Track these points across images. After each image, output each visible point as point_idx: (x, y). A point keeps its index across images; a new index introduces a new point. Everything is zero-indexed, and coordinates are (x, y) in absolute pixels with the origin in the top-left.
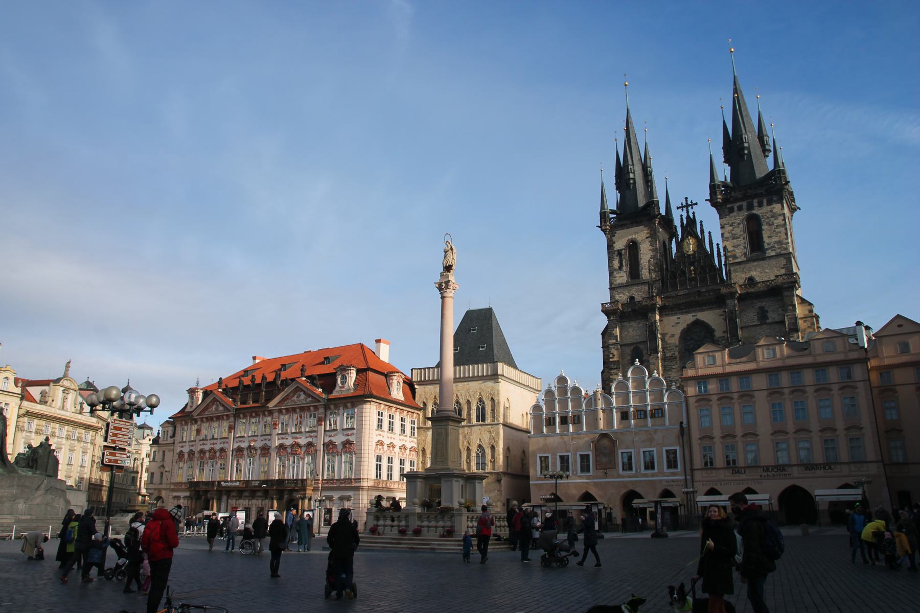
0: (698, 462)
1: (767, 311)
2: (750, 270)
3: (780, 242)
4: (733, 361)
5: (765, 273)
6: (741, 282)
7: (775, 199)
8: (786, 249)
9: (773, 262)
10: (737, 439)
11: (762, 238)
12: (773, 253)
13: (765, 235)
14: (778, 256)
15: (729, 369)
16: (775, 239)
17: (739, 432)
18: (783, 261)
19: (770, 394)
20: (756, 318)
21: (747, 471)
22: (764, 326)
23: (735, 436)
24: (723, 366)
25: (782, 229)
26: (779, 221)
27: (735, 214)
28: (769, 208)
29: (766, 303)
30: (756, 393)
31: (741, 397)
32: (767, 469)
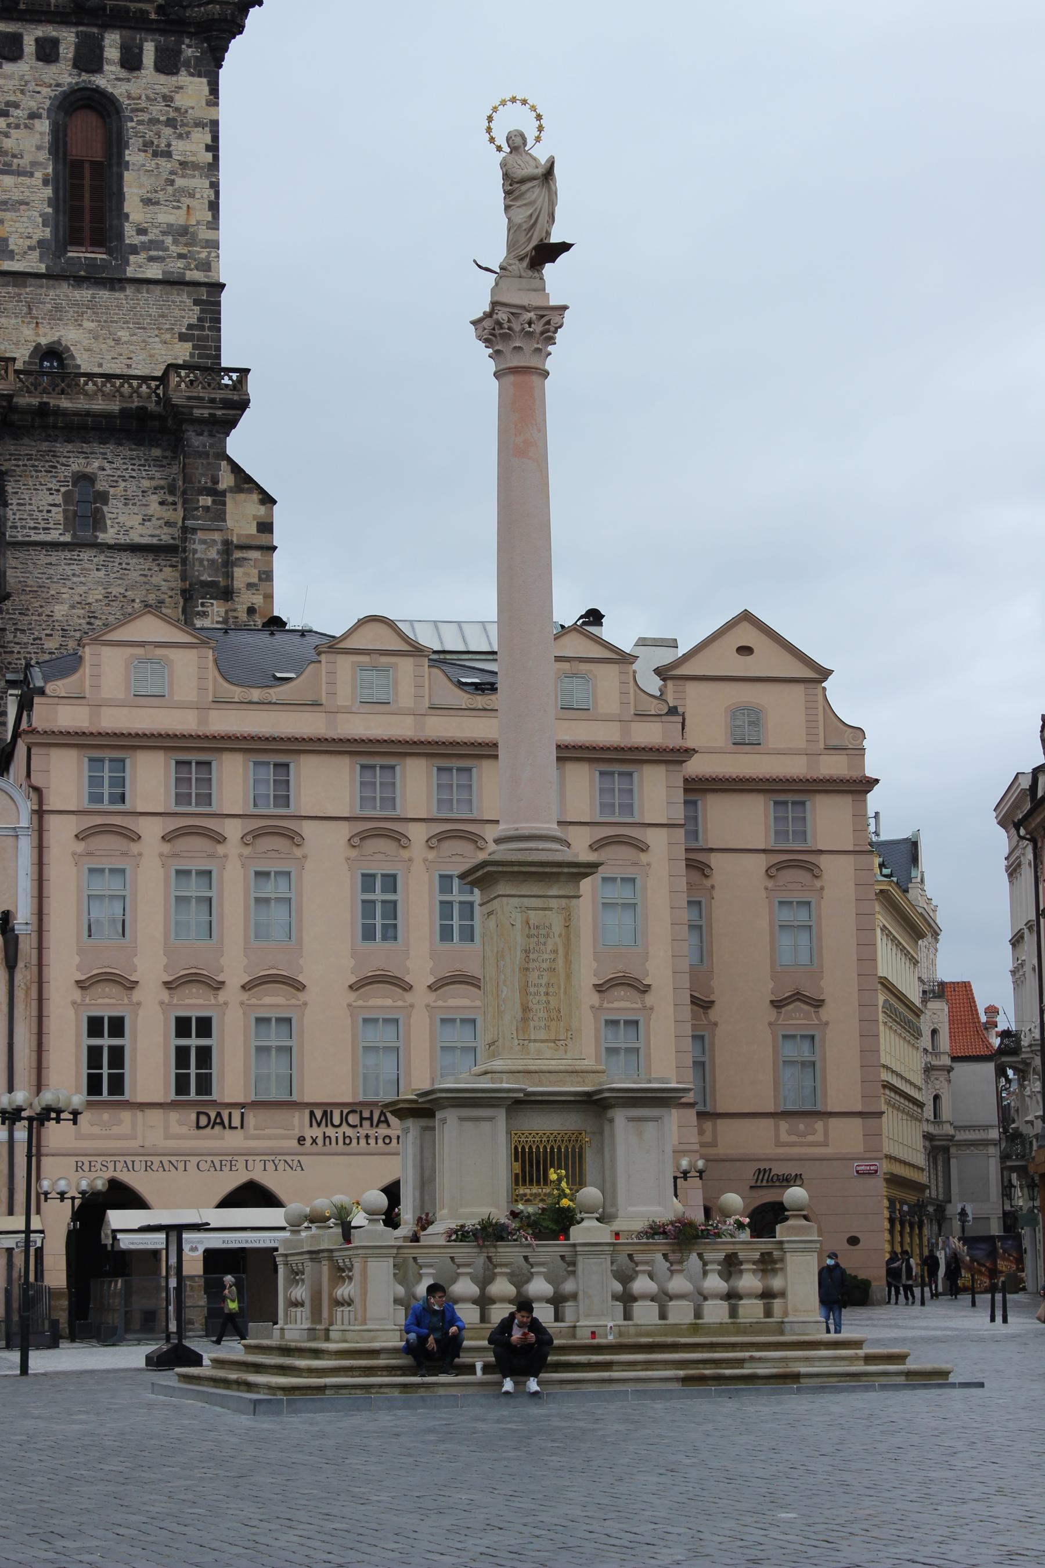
1: (103, 497)
2: (57, 313)
3: (182, 232)
4: (237, 693)
5: (117, 342)
6: (22, 355)
7: (189, 52)
8: (206, 266)
9: (149, 302)
10: (222, 996)
11: (120, 197)
12: (154, 272)
13: (134, 187)
14: (173, 282)
16: (167, 216)
17: (234, 971)
18: (185, 311)
20: (58, 514)
21: (251, 1118)
22: (86, 555)
23: (407, 988)
25: (200, 183)
26: (194, 146)
27: (25, 67)
28: (165, 82)
29: (110, 466)
30: (307, 828)
32: (322, 1114)
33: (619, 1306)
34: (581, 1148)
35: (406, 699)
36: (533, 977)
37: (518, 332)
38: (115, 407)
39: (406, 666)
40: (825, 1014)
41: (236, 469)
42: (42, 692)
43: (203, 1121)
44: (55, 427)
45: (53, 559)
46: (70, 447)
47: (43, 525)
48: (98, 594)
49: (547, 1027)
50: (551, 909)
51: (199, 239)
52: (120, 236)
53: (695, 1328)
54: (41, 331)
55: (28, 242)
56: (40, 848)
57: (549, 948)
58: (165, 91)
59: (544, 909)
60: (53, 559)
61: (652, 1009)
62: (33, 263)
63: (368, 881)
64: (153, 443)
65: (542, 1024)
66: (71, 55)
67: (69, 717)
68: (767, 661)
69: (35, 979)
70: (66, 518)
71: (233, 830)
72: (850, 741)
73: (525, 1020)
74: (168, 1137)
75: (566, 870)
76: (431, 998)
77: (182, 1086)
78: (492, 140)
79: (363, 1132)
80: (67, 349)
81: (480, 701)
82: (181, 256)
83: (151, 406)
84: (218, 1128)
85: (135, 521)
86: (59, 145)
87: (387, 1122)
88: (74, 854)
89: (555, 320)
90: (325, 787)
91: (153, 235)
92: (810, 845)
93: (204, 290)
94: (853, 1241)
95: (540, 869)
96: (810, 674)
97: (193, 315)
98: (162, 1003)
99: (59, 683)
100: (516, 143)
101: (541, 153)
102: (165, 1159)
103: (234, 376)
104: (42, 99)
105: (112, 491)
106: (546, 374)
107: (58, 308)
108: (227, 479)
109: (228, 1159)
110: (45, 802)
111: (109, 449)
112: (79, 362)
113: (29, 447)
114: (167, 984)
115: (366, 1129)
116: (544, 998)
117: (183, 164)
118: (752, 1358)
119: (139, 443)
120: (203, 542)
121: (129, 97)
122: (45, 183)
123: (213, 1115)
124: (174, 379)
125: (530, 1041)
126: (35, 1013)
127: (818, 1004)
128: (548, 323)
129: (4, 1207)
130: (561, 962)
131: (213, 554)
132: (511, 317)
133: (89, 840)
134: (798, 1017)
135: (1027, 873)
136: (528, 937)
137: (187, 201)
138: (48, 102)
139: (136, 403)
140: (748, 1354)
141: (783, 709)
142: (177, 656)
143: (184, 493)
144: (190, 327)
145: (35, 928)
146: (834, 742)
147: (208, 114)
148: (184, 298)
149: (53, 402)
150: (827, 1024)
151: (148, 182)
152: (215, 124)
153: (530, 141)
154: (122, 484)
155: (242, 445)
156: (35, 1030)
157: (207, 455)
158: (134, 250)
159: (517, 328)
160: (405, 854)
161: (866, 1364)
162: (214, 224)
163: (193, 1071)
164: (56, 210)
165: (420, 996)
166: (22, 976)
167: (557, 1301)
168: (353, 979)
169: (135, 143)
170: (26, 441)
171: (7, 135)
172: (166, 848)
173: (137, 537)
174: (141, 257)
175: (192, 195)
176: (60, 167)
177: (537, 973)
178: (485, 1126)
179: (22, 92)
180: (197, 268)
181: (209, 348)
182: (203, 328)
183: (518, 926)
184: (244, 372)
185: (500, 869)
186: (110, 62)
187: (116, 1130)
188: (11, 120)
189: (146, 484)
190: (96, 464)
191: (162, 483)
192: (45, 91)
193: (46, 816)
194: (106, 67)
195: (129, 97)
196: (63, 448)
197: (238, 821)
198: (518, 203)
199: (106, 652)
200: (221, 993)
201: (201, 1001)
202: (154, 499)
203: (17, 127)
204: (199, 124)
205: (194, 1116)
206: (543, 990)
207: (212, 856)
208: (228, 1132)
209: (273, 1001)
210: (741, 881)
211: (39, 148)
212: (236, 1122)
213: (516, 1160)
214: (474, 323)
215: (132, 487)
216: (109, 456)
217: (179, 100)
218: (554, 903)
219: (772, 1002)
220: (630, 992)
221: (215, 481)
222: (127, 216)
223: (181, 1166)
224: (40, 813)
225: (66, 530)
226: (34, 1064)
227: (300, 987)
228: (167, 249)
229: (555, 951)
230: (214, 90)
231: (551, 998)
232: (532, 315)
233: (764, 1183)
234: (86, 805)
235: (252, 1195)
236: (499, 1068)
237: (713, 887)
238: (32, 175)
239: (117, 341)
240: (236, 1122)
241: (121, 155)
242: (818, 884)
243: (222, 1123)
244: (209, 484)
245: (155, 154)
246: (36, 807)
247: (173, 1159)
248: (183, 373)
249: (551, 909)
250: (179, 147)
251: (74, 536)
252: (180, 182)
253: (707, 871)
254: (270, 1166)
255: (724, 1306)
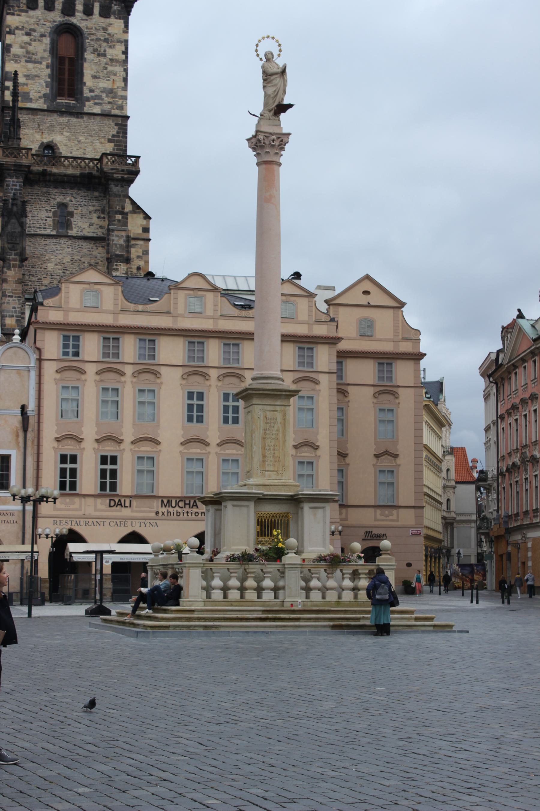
0: (50, 483)
1: (71, 214)
3: (111, 92)
4: (132, 307)
5: (78, 142)
6: (35, 147)
7: (115, 8)
8: (121, 108)
9: (94, 124)
10: (122, 446)
11: (82, 74)
12: (97, 110)
13: (88, 70)
15: (126, 320)
16: (103, 84)
17: (128, 434)
19: (186, 376)
20: (50, 221)
21: (134, 503)
22: (63, 241)
23: (207, 444)
24: (113, 313)
25: (119, 69)
26: (116, 52)
28: (103, 22)
29: (74, 200)
31: (137, 374)
32: (167, 501)
33: (304, 593)
34: (288, 520)
35: (209, 312)
36: (268, 442)
37: (267, 145)
38: (77, 172)
39: (210, 296)
40: (398, 461)
41: (133, 203)
42: (42, 304)
43: (112, 503)
44: (49, 181)
45: (47, 242)
46: (56, 190)
47: (43, 226)
48: (68, 259)
49: (274, 465)
50: (276, 411)
51: (118, 95)
52: (82, 93)
53: (338, 603)
54: (44, 136)
55: (39, 95)
56: (40, 376)
57: (276, 428)
58: (104, 25)
59: (274, 411)
60: (47, 242)
61: (319, 457)
62: (40, 104)
63: (190, 395)
64: (95, 190)
65: (271, 463)
66: (60, 8)
67: (54, 316)
68: (376, 298)
69: (36, 436)
70: (54, 223)
71: (129, 370)
72: (414, 336)
73: (264, 461)
74: (96, 510)
75: (284, 393)
76: (218, 449)
77: (103, 487)
78: (258, 55)
79: (185, 510)
80: (56, 145)
81: (244, 313)
82: (110, 103)
83: (95, 172)
84: (119, 507)
85: (86, 226)
86: (54, 50)
87: (197, 506)
88: (55, 379)
89: (285, 139)
90: (171, 351)
91: (97, 92)
92: (394, 383)
93: (120, 119)
94: (409, 565)
95: (272, 393)
96: (395, 304)
97: (114, 130)
98: (94, 449)
99: (50, 300)
100: (269, 57)
101: (280, 62)
102: (95, 520)
103: (133, 159)
104: (47, 28)
105: (75, 211)
106: (280, 164)
107: (52, 126)
108: (128, 208)
109: (124, 520)
110: (42, 355)
111: (74, 192)
112: (61, 151)
113: (37, 190)
114: (97, 441)
115: (187, 509)
116: (273, 452)
117: (111, 60)
118: (364, 618)
119: (88, 189)
120: (117, 236)
121: (87, 28)
122: (47, 67)
123: (117, 501)
124: (105, 160)
125: (266, 471)
126: (36, 452)
127: (396, 456)
128: (282, 141)
129: (20, 541)
130: (281, 435)
131: (122, 242)
132: (265, 138)
133: (62, 373)
134: (386, 463)
135: (493, 398)
136: (266, 423)
137: (113, 77)
138: (49, 29)
139: (87, 171)
140: (362, 616)
141: (383, 321)
142: (104, 288)
143: (109, 213)
144: (113, 136)
145: (37, 413)
146: (406, 336)
147: (123, 37)
148: (110, 122)
149: (49, 169)
150: (399, 465)
151: (95, 68)
152: (126, 42)
153: (275, 56)
154: (80, 208)
155: (135, 191)
156: (36, 460)
157: (120, 196)
158: (88, 99)
159: (267, 143)
160: (208, 383)
161: (415, 621)
162: (125, 88)
163: (108, 480)
164: (52, 80)
165: (213, 449)
166: (30, 435)
167: (276, 590)
168: (183, 440)
169: (89, 49)
170: (36, 187)
171: (30, 44)
172: (98, 378)
173: (86, 233)
174: (91, 103)
175: (115, 75)
176: (55, 60)
177: (269, 440)
178: (245, 510)
179: (37, 24)
180: (117, 109)
181: (122, 146)
182: (119, 137)
183: (262, 418)
184: (138, 158)
185: (254, 392)
186: (78, 11)
187: (72, 507)
188: (32, 37)
189: (91, 208)
190: (68, 199)
191: (99, 208)
192: (48, 24)
193: (43, 362)
194: (77, 14)
195: (87, 28)
196: (53, 191)
197: (131, 366)
198: (270, 85)
199: (72, 286)
200: (122, 445)
201: (112, 448)
202: (95, 216)
203: (35, 40)
204: (119, 41)
205: (108, 501)
206: (272, 448)
207: (119, 382)
208: (123, 509)
209: (146, 449)
210: (362, 400)
211: (45, 51)
212: (127, 504)
213: (258, 525)
214: (248, 140)
215: (85, 209)
216: (74, 195)
217: (111, 30)
218: (278, 408)
219: (375, 455)
220: (310, 449)
221: (123, 208)
222: (85, 83)
223: (102, 524)
224: (40, 360)
225: (54, 229)
226: (35, 476)
227: (158, 443)
228: (103, 99)
229: (278, 430)
230: (127, 26)
231: (275, 452)
232: (274, 137)
233: (369, 538)
234: (61, 357)
235: (134, 538)
236: (251, 483)
237: (349, 401)
238: (41, 63)
239: (79, 142)
240: (127, 504)
241: (83, 55)
242: (397, 401)
243: (121, 505)
244: (120, 209)
245: (99, 55)
246: (38, 357)
247: (99, 520)
248: (109, 157)
249: (276, 411)
250: (110, 52)
251: (57, 232)
252: (110, 68)
253: (346, 394)
254: (143, 524)
255: (351, 593)
